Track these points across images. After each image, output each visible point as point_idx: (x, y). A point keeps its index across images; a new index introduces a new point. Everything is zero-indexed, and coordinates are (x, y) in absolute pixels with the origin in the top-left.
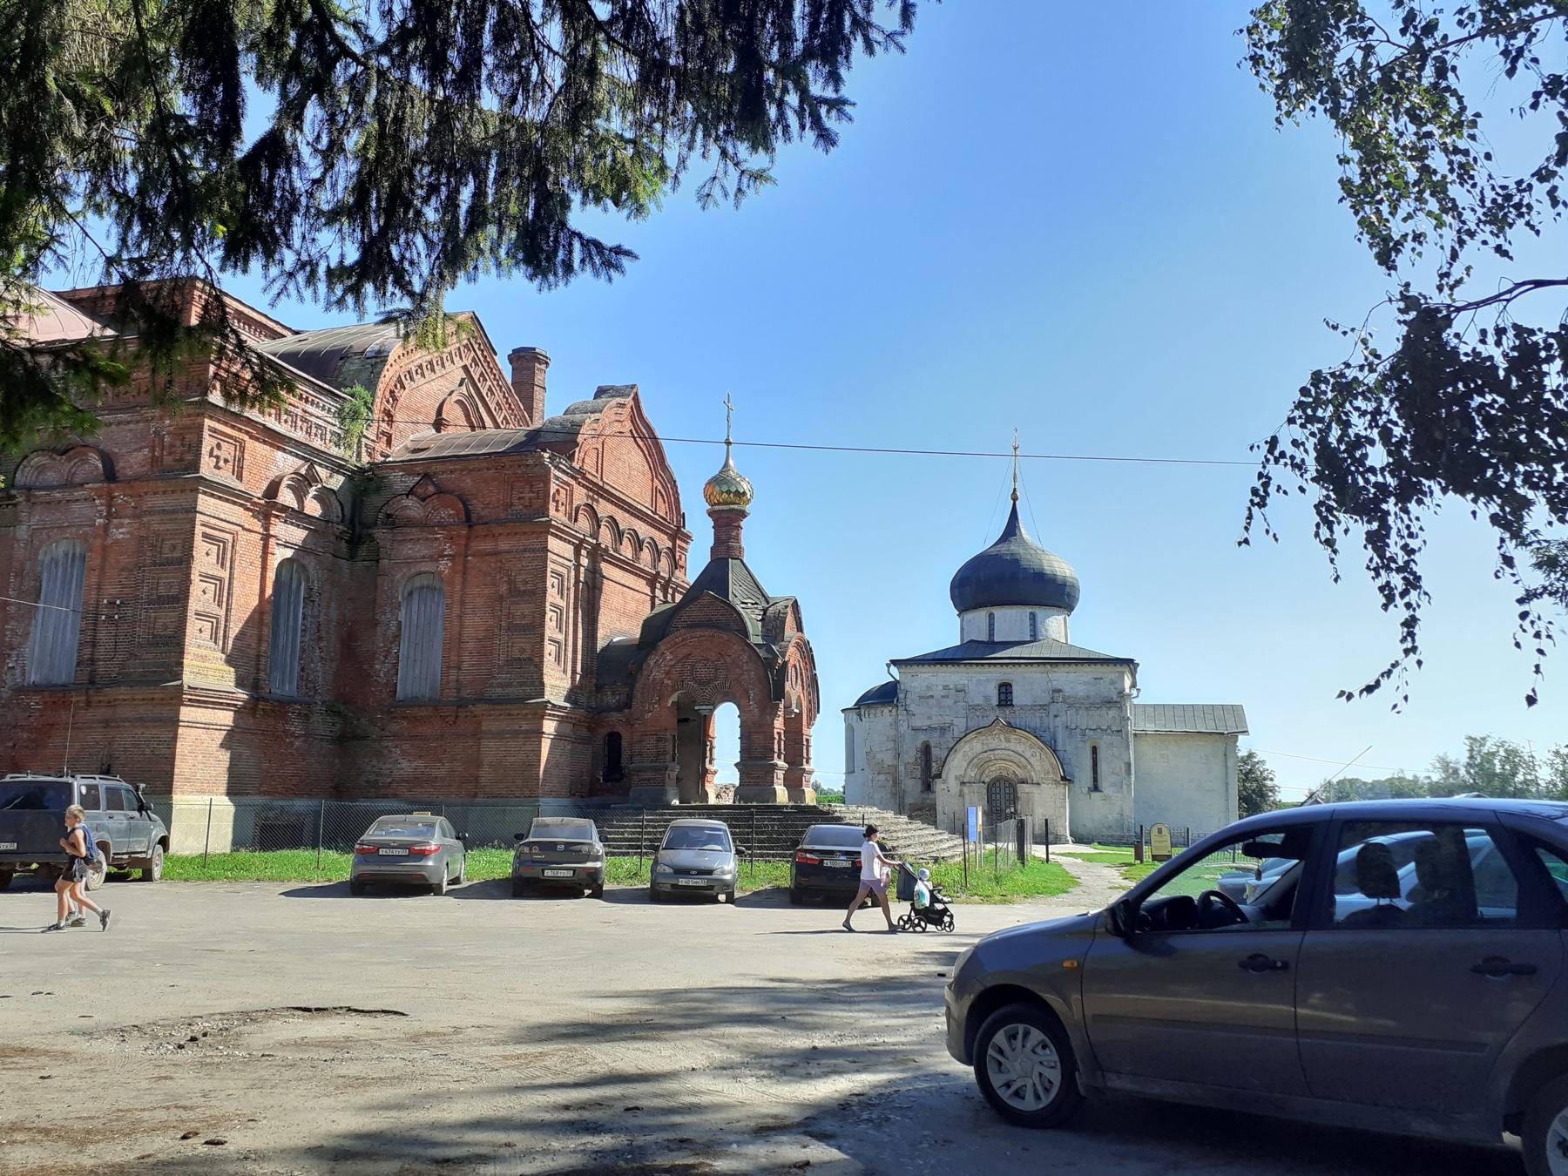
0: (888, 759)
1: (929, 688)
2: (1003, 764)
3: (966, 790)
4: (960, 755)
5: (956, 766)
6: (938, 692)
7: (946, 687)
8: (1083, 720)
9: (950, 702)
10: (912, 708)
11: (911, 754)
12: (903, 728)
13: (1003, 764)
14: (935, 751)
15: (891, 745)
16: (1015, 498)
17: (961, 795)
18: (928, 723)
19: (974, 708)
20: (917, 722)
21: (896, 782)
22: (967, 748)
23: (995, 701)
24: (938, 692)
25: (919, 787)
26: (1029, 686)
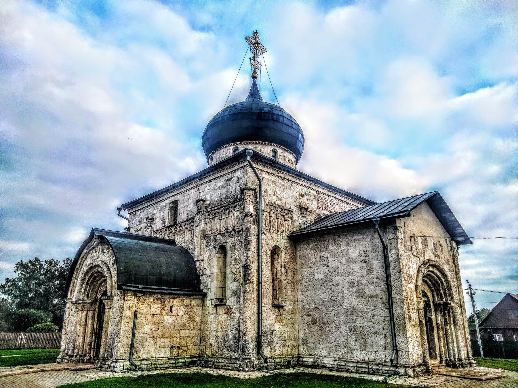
8: (217, 225)
16: (254, 77)
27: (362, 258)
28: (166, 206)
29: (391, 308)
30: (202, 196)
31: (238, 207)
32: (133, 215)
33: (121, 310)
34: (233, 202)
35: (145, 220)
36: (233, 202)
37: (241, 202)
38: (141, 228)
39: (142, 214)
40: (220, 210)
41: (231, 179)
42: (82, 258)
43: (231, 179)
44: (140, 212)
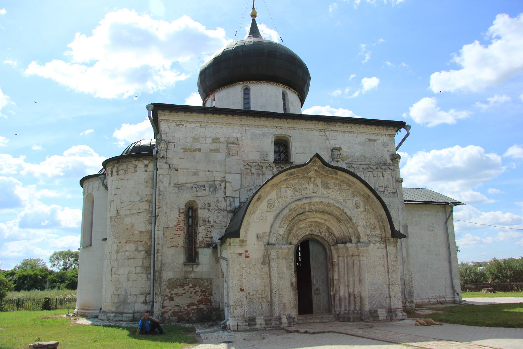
0: (140, 223)
1: (196, 140)
2: (316, 217)
3: (273, 254)
4: (263, 205)
5: (258, 224)
6: (205, 145)
7: (215, 140)
9: (220, 156)
10: (175, 161)
11: (171, 216)
12: (164, 184)
13: (316, 217)
14: (202, 214)
15: (144, 206)
17: (266, 260)
18: (195, 179)
19: (248, 164)
20: (182, 179)
21: (150, 252)
22: (273, 195)
23: (272, 157)
24: (205, 145)
25: (182, 258)
26: (304, 145)
27: (431, 228)
28: (264, 135)
29: (450, 262)
30: (334, 144)
31: (388, 170)
32: (173, 124)
33: (393, 259)
34: (384, 164)
35: (209, 140)
36: (384, 164)
37: (392, 167)
38: (199, 150)
39: (203, 130)
40: (365, 167)
41: (375, 140)
42: (272, 185)
43: (375, 140)
44: (193, 125)
